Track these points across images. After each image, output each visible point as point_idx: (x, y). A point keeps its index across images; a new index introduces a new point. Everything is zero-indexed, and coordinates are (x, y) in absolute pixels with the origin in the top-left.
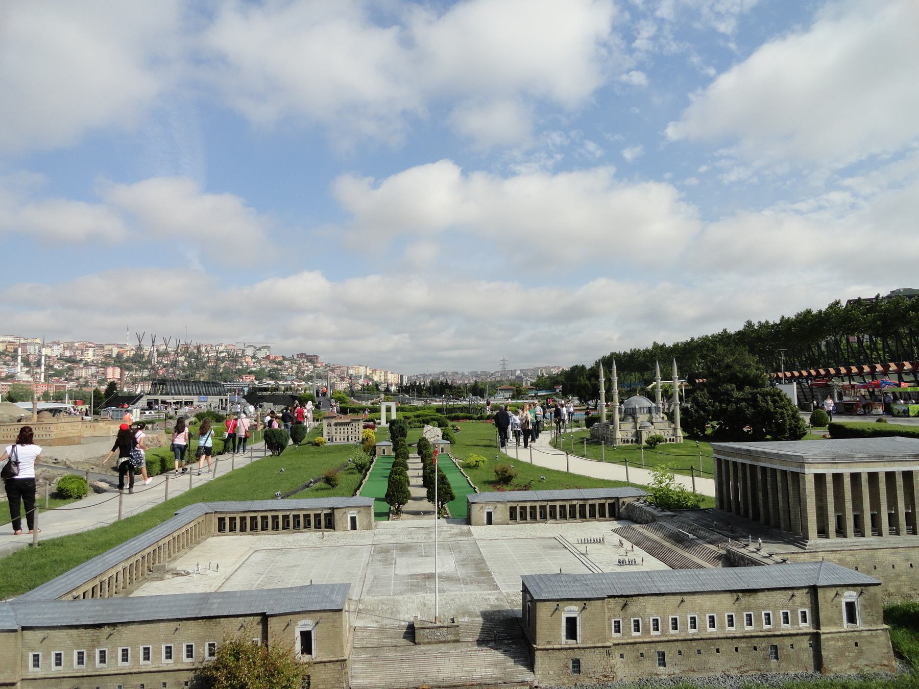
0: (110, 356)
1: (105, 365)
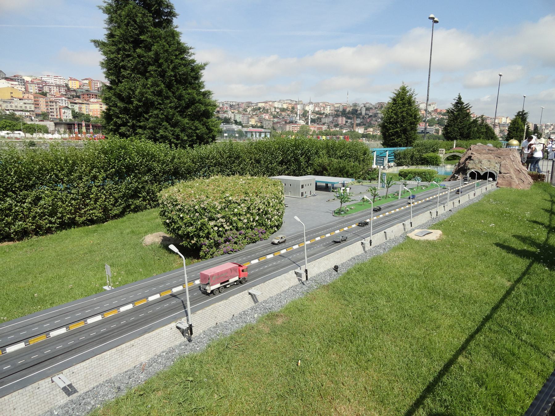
0: (338, 111)
1: (337, 116)
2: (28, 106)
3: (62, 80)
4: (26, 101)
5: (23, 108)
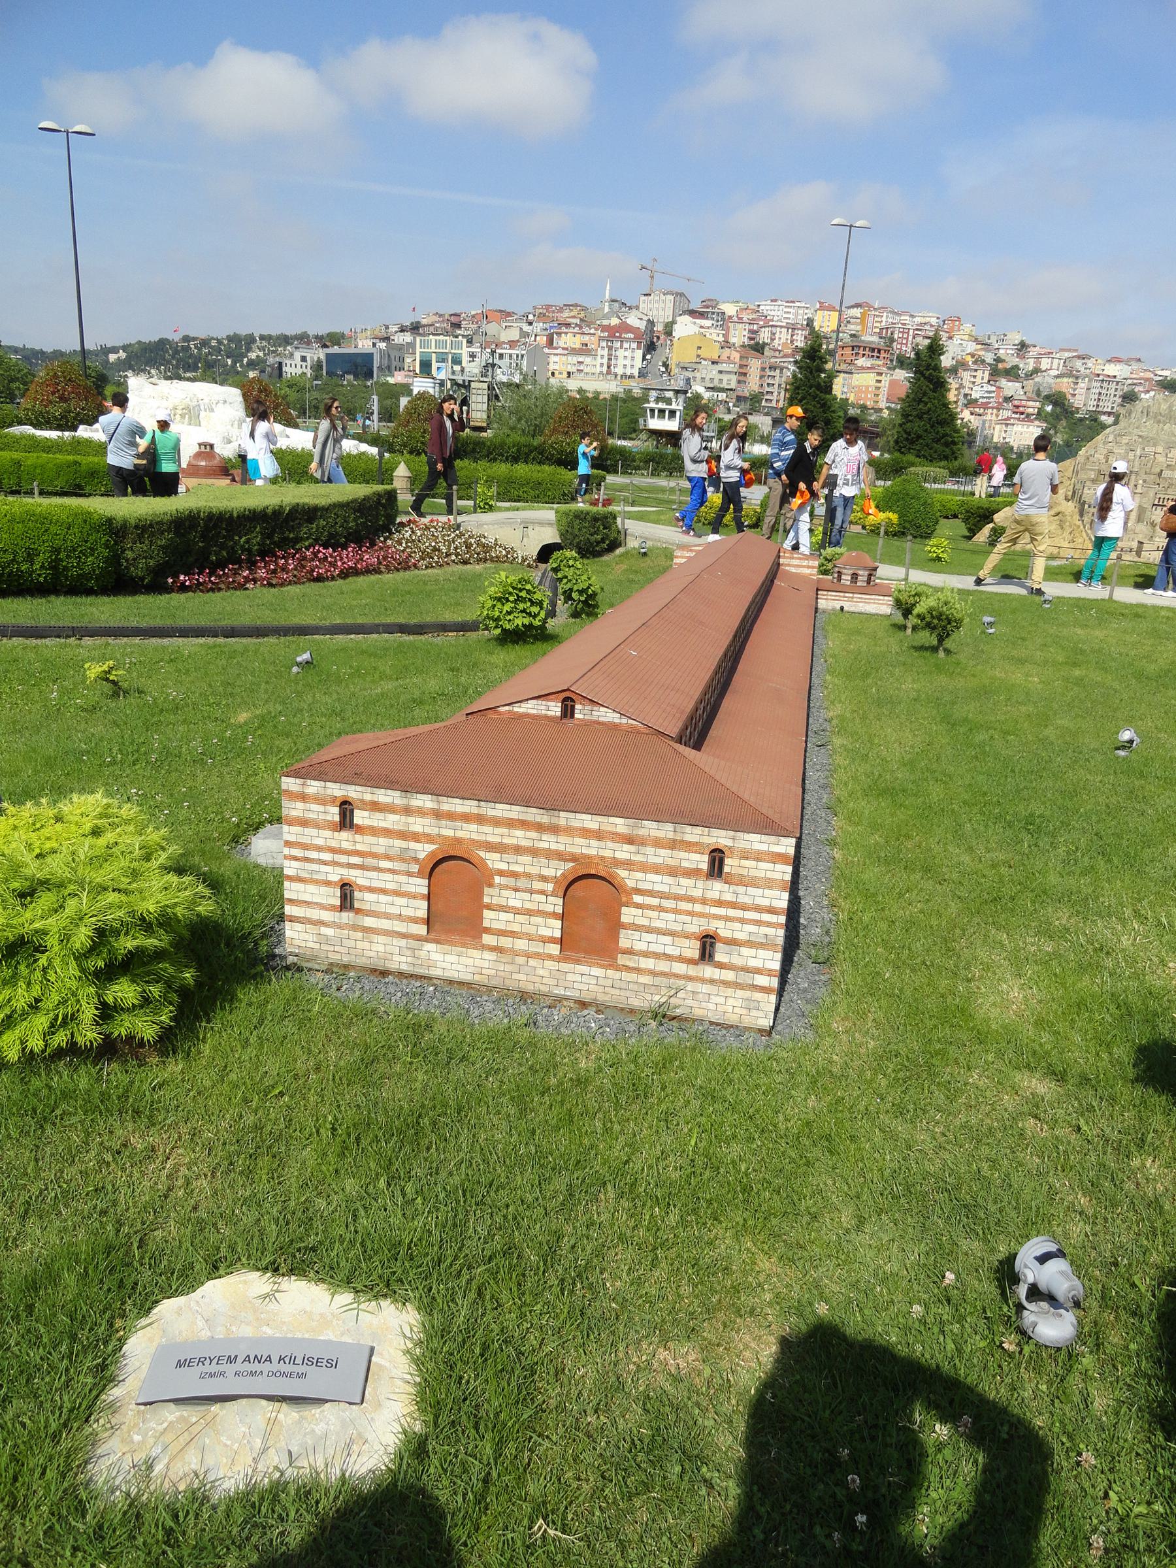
2: (725, 377)
3: (801, 311)
4: (723, 367)
5: (716, 383)
